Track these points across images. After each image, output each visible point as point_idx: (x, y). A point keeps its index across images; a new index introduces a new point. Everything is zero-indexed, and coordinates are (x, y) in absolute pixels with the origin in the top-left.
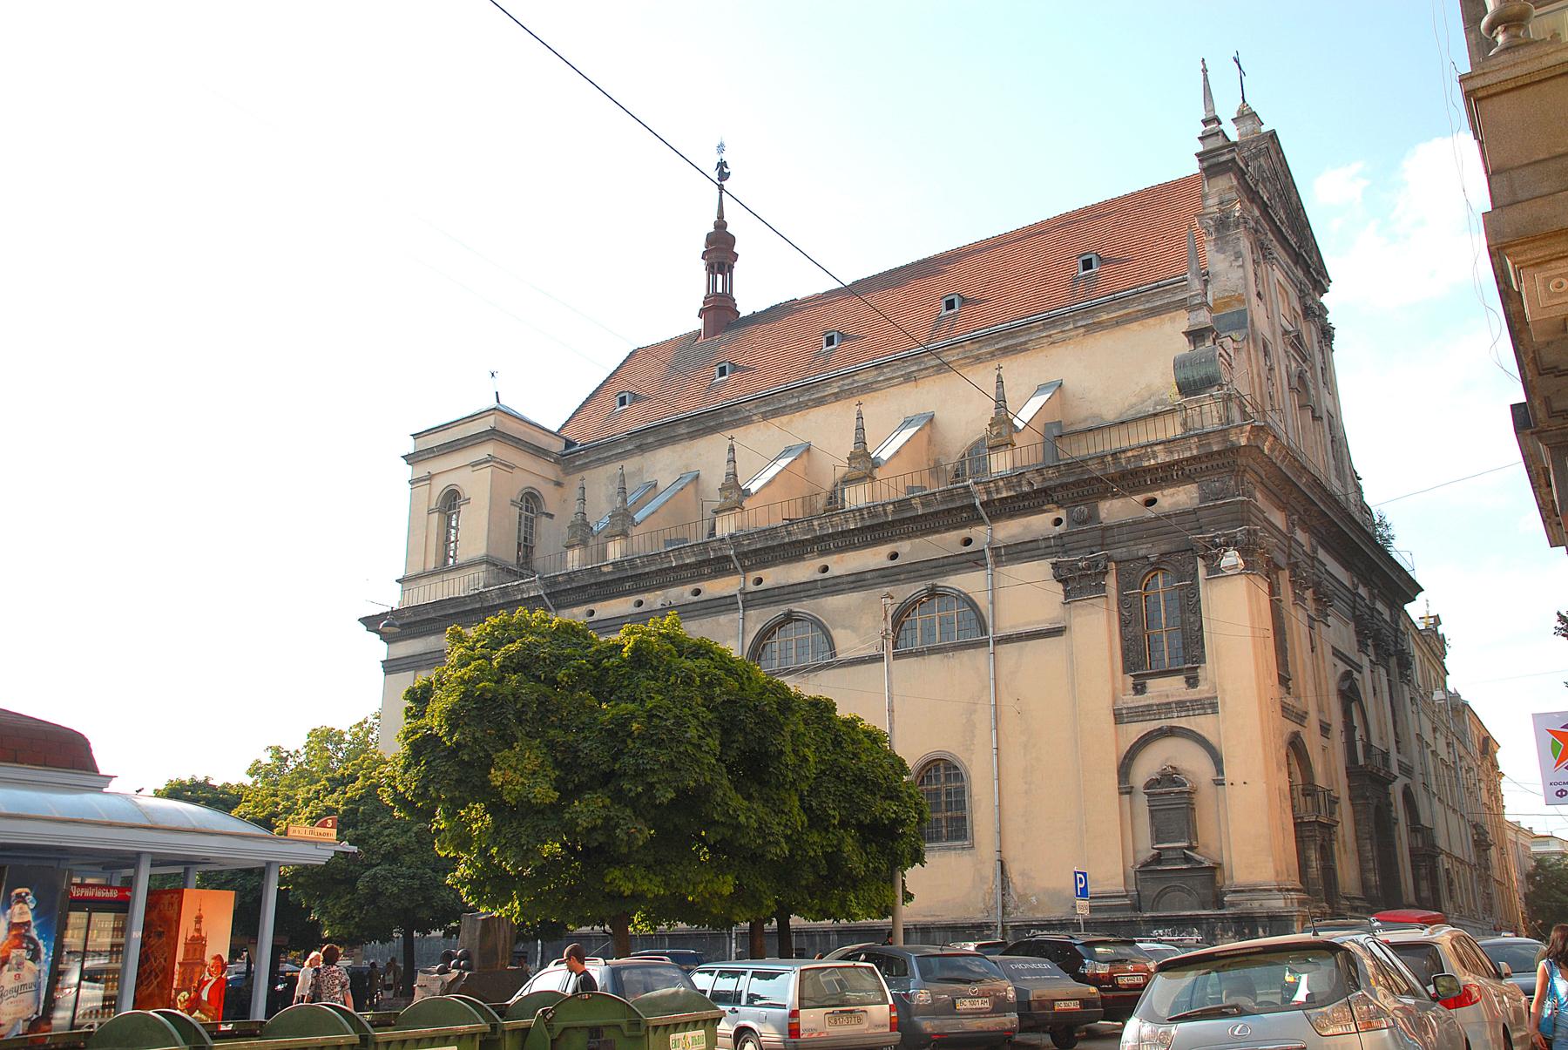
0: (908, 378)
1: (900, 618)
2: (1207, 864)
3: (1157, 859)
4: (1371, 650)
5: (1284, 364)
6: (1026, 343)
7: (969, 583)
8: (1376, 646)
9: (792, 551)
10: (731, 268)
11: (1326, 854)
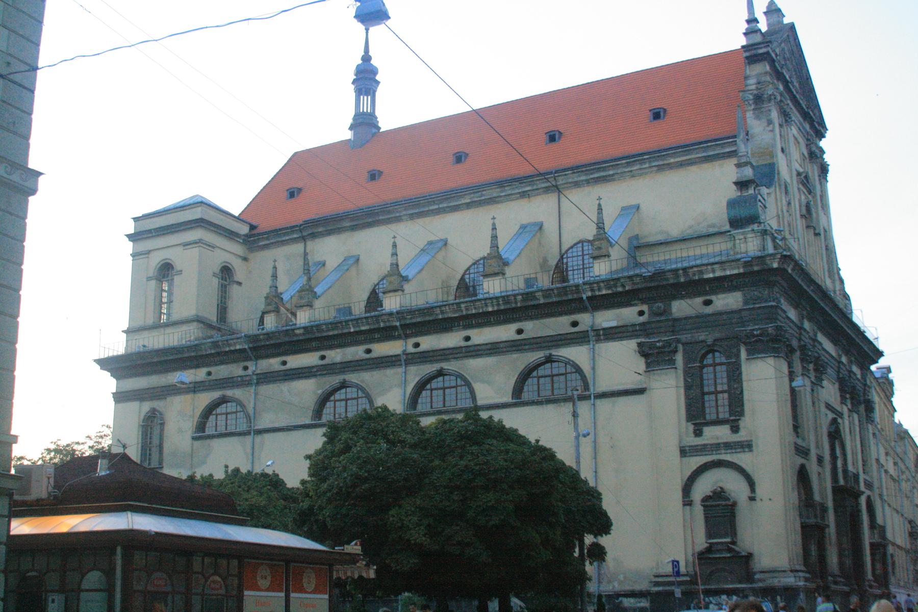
0: (524, 195)
1: (525, 376)
2: (743, 554)
3: (709, 550)
4: (849, 402)
5: (798, 197)
6: (613, 175)
7: (577, 354)
8: (852, 398)
9: (444, 325)
10: (374, 92)
11: (822, 548)
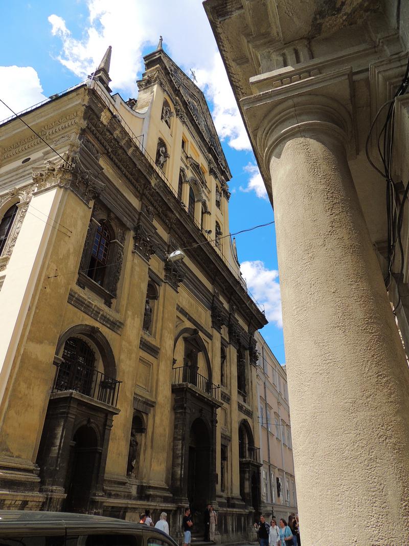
8: (230, 333)
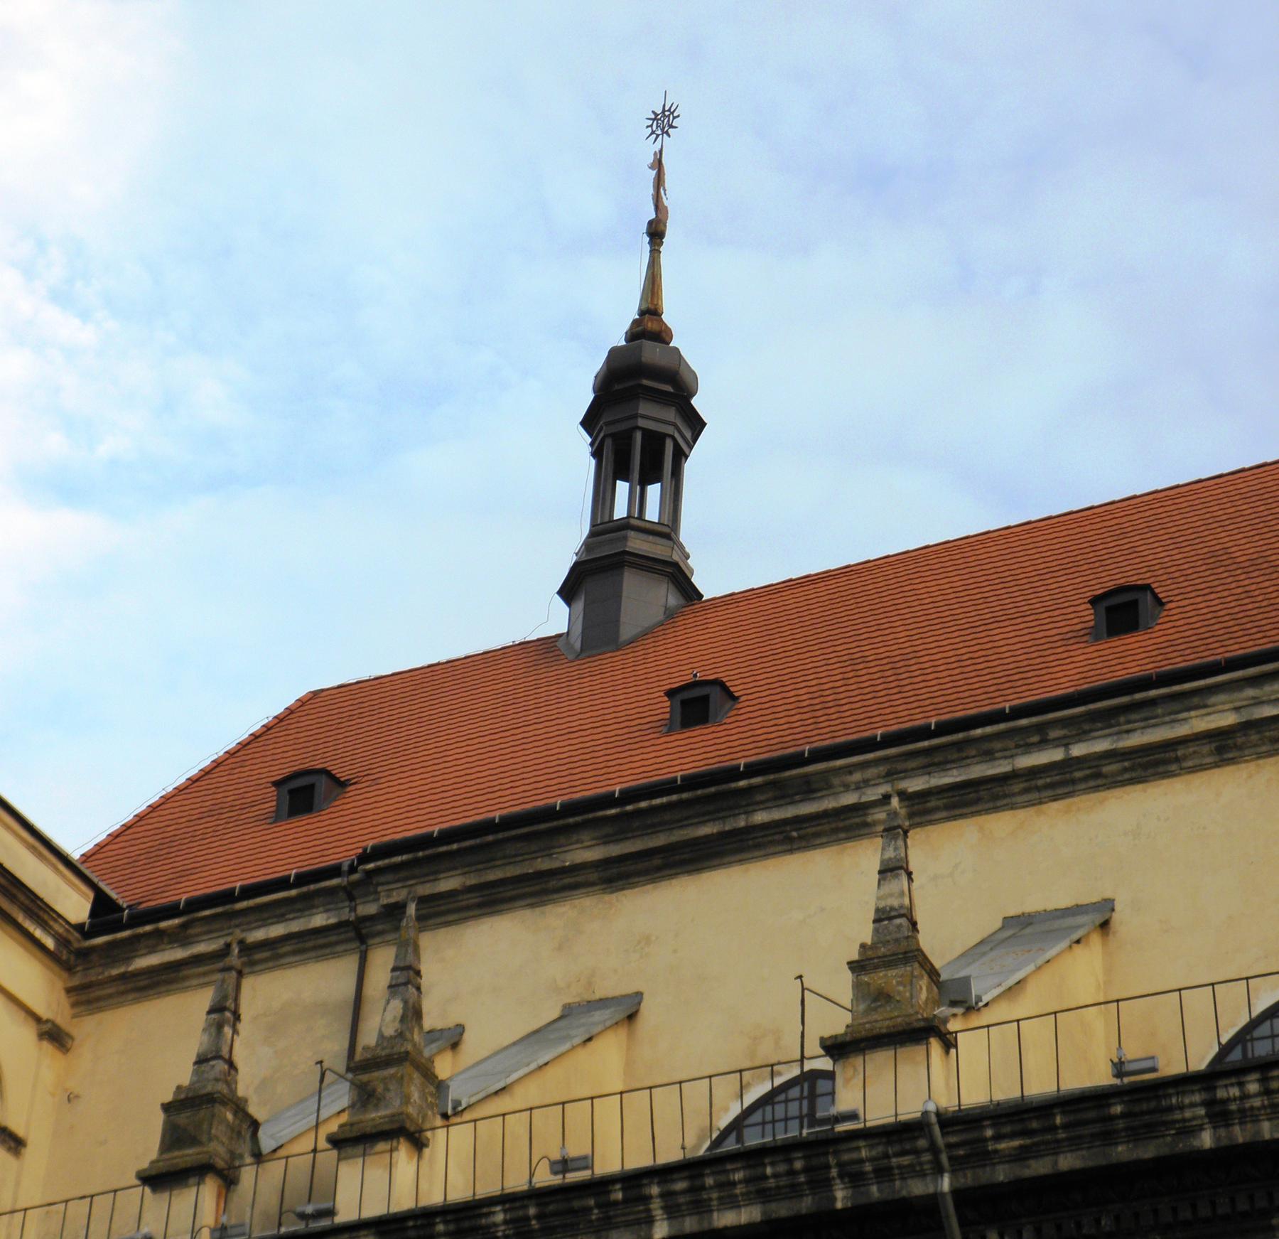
10: (680, 456)
